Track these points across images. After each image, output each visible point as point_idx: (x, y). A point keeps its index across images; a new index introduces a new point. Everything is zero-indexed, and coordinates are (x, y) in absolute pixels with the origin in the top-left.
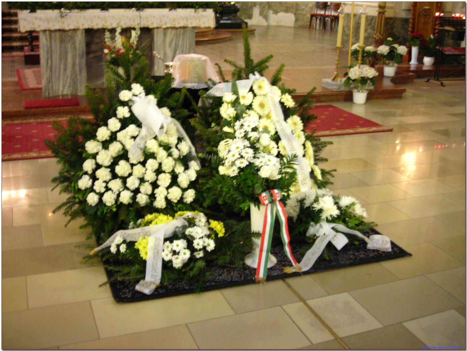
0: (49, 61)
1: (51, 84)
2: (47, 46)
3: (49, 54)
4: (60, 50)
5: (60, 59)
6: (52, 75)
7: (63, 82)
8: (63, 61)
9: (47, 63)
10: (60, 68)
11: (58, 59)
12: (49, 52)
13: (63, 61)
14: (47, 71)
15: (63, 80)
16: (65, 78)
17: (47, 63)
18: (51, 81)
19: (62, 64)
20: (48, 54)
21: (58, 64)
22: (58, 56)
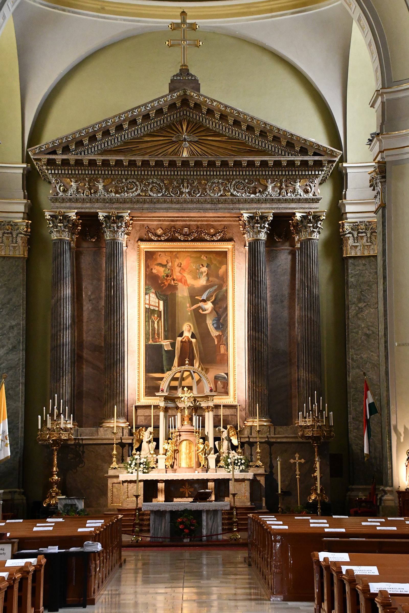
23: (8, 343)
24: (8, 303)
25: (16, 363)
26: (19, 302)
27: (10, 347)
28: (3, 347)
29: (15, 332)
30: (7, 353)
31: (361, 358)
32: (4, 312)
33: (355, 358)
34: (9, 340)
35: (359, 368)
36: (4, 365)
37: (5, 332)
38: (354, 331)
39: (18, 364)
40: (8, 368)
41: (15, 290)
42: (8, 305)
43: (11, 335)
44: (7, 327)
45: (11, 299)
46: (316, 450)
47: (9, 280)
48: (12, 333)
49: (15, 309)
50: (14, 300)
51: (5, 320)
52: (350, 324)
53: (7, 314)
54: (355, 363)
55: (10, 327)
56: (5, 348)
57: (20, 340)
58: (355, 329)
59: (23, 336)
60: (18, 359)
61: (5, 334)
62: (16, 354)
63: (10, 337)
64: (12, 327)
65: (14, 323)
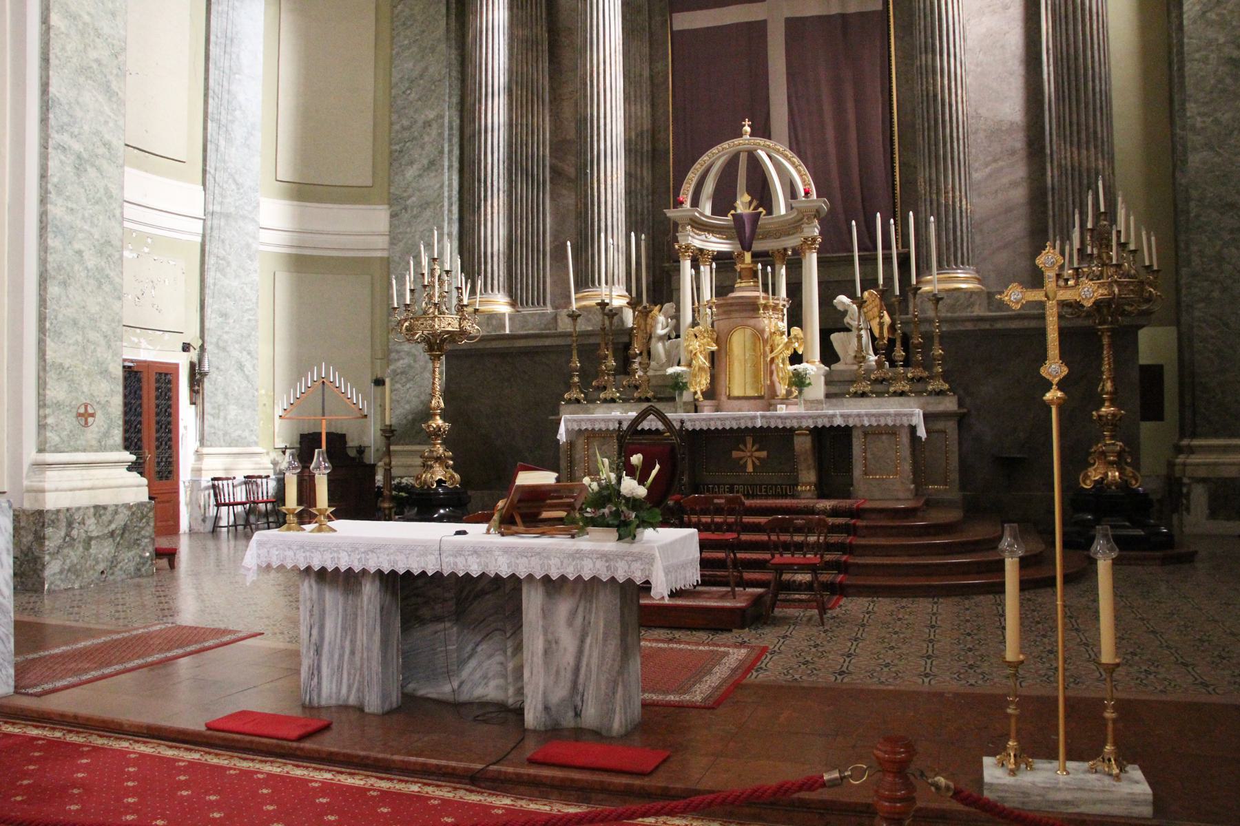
0: (315, 632)
1: (316, 679)
2: (311, 600)
3: (316, 616)
4: (345, 610)
5: (344, 629)
6: (319, 660)
7: (349, 680)
8: (349, 633)
9: (310, 635)
10: (342, 647)
11: (339, 630)
12: (316, 611)
13: (349, 633)
14: (308, 651)
15: (349, 674)
16: (353, 671)
17: (310, 635)
18: (316, 673)
19: (349, 638)
20: (311, 615)
21: (338, 641)
22: (340, 619)
23: (420, 155)
24: (421, 76)
25: (436, 194)
26: (439, 74)
27: (425, 162)
28: (411, 163)
29: (434, 133)
30: (420, 176)
31: (1217, 122)
32: (413, 95)
33: (1199, 125)
34: (423, 148)
35: (1212, 148)
36: (414, 199)
37: (416, 134)
38: (1197, 56)
39: (439, 195)
40: (421, 206)
41: (433, 50)
42: (422, 82)
43: (426, 139)
44: (420, 123)
45: (426, 68)
46: (1105, 341)
47: (424, 31)
48: (428, 134)
49: (433, 87)
50: (431, 70)
51: (416, 111)
52: (1186, 40)
53: (420, 99)
54: (1200, 138)
55: (424, 123)
56: (415, 167)
57: (443, 147)
58: (1198, 51)
59: (450, 140)
60: (438, 185)
61: (414, 139)
62: (436, 176)
63: (424, 144)
64: (427, 124)
65: (431, 115)
